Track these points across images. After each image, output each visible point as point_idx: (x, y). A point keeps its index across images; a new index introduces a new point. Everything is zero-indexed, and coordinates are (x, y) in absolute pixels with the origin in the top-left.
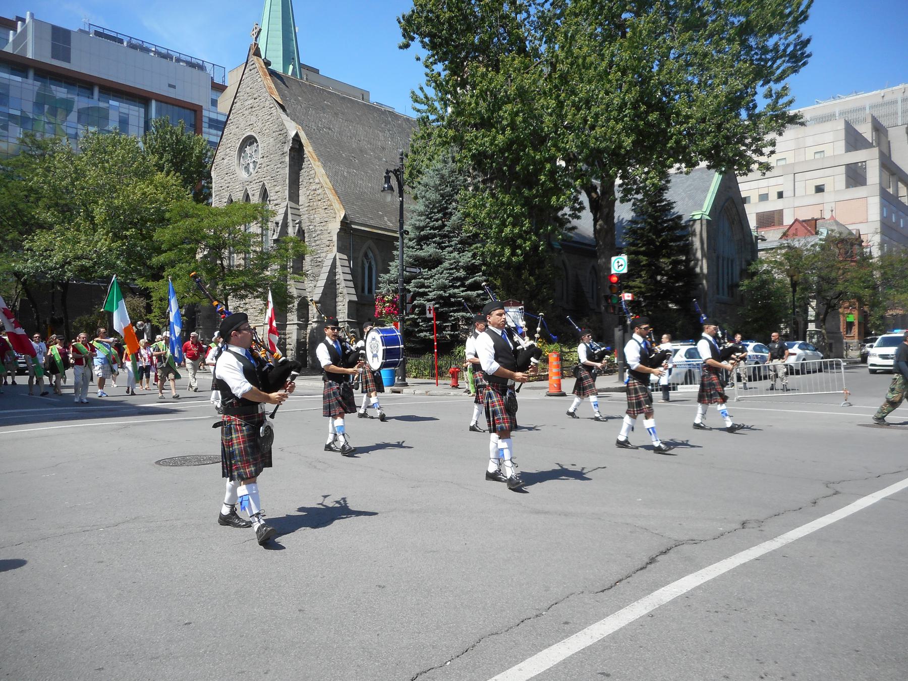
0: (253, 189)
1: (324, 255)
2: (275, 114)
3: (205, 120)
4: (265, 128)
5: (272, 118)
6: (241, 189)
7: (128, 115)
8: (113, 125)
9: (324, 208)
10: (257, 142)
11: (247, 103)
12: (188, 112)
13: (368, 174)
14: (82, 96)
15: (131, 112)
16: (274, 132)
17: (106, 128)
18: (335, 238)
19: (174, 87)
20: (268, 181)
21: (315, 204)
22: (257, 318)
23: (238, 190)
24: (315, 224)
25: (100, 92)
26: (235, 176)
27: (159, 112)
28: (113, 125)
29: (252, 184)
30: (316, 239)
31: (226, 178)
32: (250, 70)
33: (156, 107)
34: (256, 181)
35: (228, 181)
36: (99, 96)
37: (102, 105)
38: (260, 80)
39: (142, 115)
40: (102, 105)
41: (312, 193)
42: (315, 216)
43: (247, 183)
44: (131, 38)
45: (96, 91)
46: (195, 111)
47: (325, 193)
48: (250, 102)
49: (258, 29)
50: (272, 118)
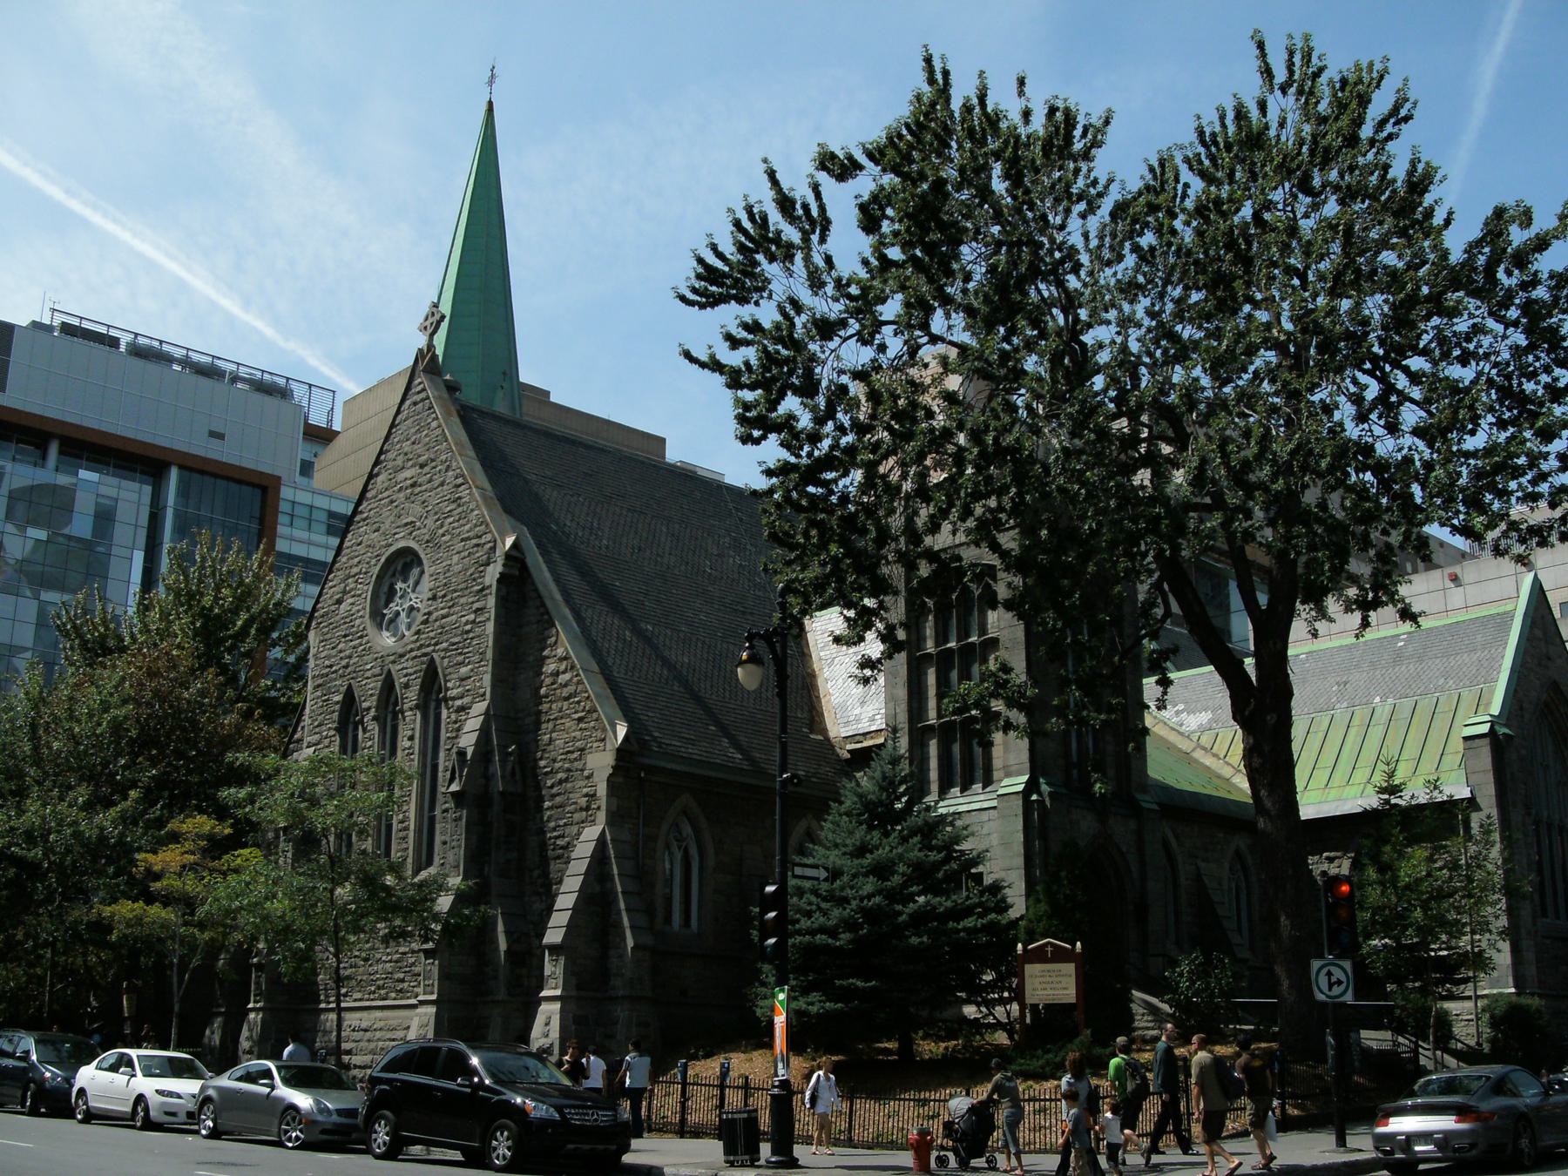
1: (574, 829)
3: (284, 507)
4: (441, 531)
5: (460, 509)
6: (377, 671)
7: (117, 500)
8: (81, 526)
9: (576, 716)
10: (420, 563)
11: (401, 476)
12: (246, 490)
13: (681, 635)
14: (21, 461)
15: (123, 494)
17: (66, 531)
18: (602, 790)
19: (221, 436)
20: (442, 654)
21: (554, 706)
22: (400, 986)
23: (368, 674)
25: (61, 452)
27: (183, 492)
28: (81, 526)
30: (555, 790)
31: (341, 646)
32: (415, 404)
33: (181, 480)
34: (414, 654)
35: (347, 653)
36: (58, 461)
37: (63, 480)
38: (434, 424)
39: (147, 499)
40: (63, 480)
42: (554, 735)
44: (136, 335)
45: (53, 450)
46: (264, 489)
47: (580, 682)
48: (408, 473)
49: (437, 317)
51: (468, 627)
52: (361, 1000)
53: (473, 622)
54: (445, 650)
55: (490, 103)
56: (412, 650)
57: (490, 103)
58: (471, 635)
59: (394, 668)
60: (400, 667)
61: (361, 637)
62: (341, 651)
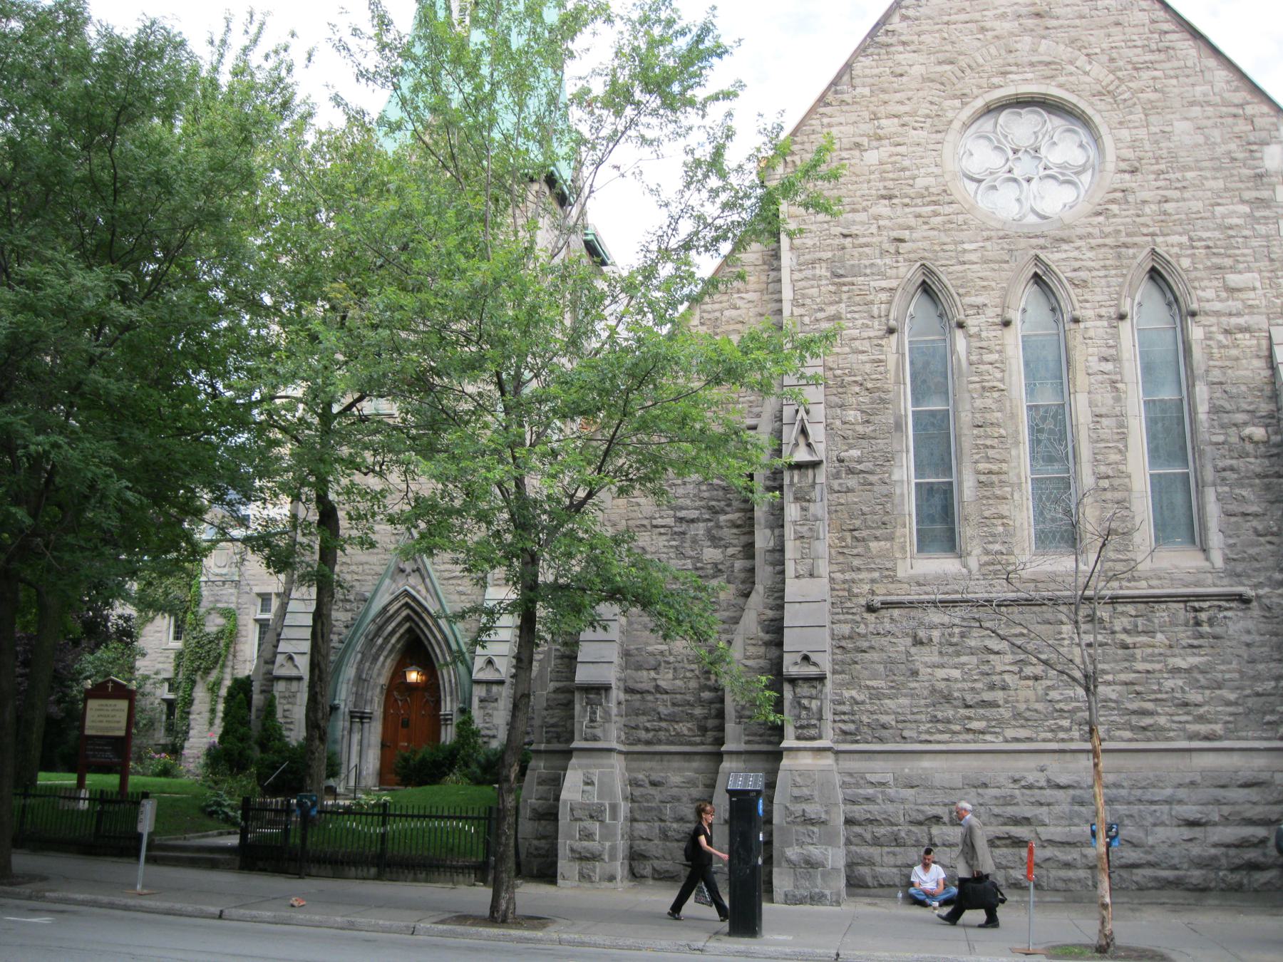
0: (1077, 264)
2: (1193, 52)
5: (1175, 64)
16: (1192, 104)
20: (1176, 250)
23: (973, 257)
26: (948, 209)
29: (1065, 246)
43: (1041, 241)
50: (1175, 64)
51: (1235, 221)
52: (1029, 739)
53: (1250, 216)
54: (1180, 245)
56: (1090, 235)
59: (1050, 257)
60: (1064, 255)
61: (935, 203)
62: (877, 217)
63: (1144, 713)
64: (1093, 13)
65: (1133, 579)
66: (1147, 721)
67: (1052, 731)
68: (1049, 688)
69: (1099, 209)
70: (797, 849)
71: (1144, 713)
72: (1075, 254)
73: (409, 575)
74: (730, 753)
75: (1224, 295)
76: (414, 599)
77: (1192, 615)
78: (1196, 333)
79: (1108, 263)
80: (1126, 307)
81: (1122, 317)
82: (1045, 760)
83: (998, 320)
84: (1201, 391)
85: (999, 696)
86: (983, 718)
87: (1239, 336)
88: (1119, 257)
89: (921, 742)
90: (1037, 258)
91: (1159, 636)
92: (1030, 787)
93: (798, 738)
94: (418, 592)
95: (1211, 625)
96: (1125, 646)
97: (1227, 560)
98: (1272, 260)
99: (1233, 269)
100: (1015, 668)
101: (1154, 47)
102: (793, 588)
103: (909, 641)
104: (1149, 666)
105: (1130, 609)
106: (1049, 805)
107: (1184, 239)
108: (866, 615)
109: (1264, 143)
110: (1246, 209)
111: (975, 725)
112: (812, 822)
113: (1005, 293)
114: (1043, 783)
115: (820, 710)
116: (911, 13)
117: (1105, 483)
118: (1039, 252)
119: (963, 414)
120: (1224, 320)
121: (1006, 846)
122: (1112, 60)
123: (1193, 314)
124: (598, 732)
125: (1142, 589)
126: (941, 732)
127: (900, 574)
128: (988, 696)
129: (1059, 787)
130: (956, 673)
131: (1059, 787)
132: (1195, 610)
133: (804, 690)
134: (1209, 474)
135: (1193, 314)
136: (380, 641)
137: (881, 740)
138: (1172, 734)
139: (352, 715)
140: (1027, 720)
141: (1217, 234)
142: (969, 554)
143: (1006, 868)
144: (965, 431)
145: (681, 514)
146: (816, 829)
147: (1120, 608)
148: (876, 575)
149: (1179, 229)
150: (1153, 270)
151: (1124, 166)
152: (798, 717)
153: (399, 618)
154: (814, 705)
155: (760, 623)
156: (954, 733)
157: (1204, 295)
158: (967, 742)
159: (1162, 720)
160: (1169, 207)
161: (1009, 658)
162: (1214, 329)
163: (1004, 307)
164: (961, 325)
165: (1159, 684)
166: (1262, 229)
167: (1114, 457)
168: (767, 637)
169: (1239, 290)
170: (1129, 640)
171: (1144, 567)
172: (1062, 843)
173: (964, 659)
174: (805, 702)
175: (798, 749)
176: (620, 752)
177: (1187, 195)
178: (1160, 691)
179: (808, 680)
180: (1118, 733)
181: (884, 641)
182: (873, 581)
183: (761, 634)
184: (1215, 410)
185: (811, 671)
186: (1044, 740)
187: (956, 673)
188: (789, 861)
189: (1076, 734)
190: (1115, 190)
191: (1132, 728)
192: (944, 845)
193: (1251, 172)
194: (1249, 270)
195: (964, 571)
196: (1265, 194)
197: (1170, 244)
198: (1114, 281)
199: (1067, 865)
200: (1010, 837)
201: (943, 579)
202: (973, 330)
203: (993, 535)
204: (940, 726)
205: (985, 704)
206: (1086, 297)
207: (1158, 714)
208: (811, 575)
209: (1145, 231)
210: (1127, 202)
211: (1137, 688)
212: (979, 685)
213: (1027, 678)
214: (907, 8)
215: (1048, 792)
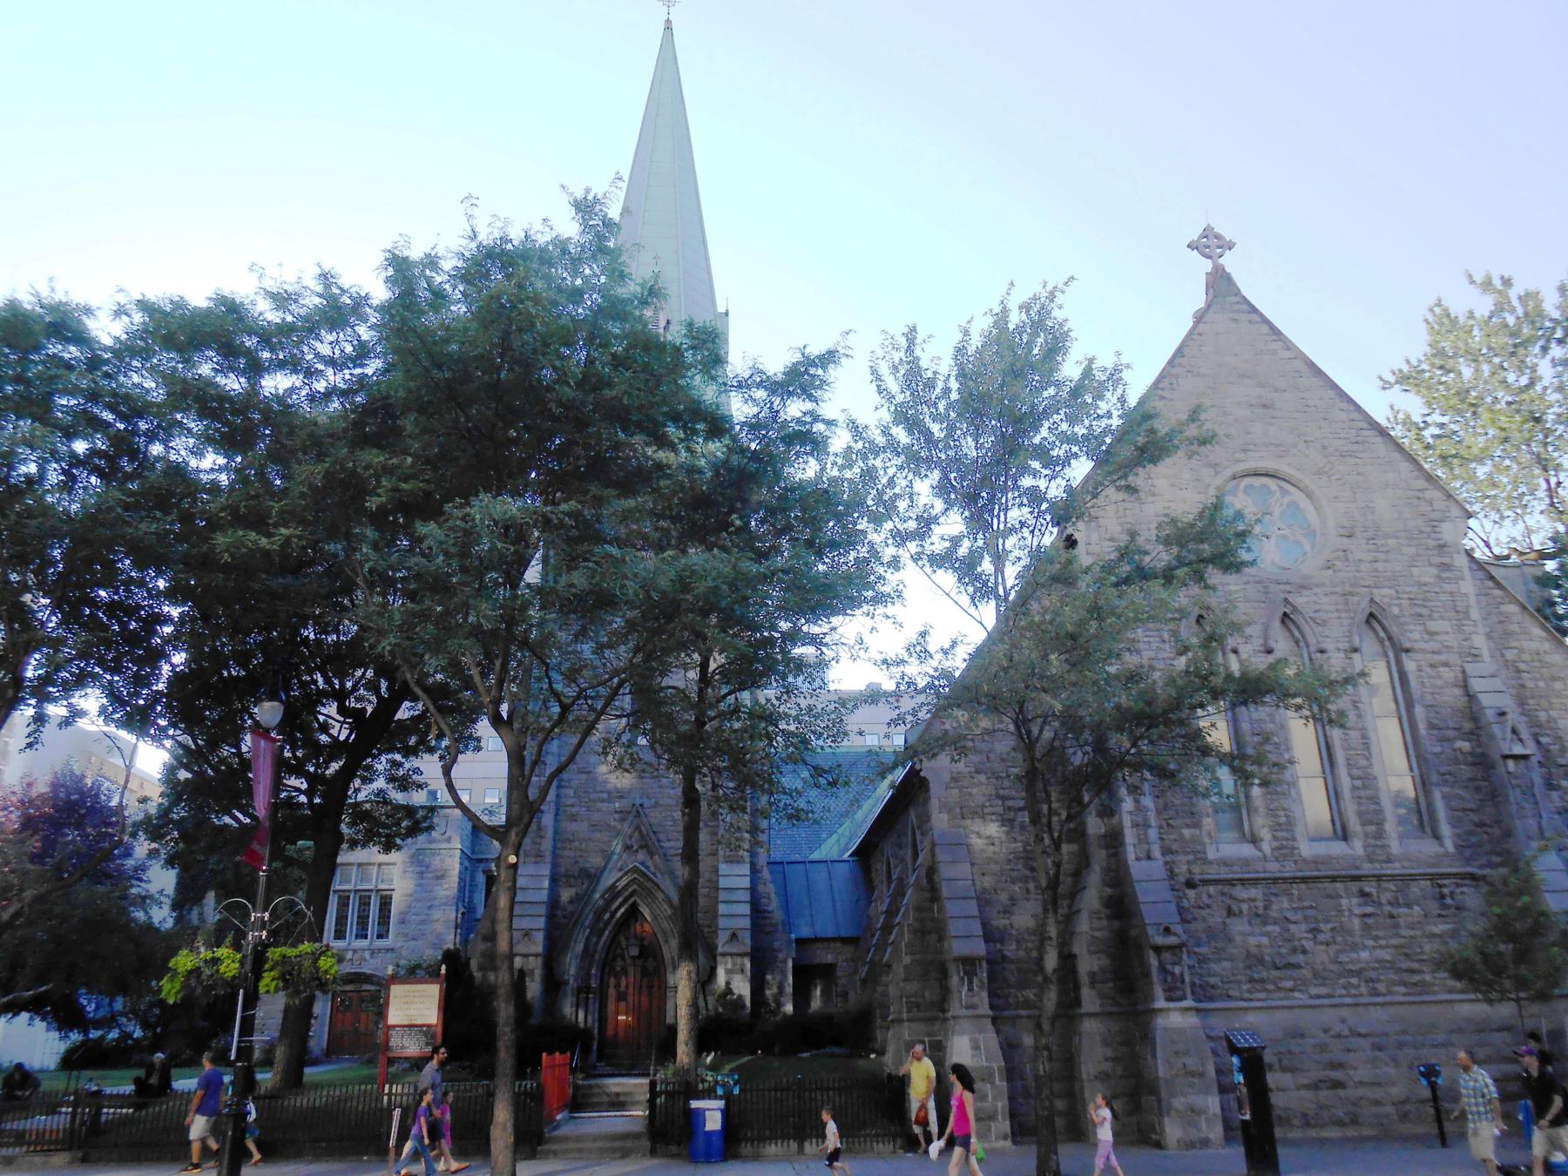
0: (1317, 607)
20: (1386, 600)
24: (1560, 733)
29: (1306, 592)
32: (1236, 320)
41: (1526, 657)
43: (1288, 588)
55: (668, 21)
56: (1323, 584)
57: (668, 21)
58: (1437, 589)
59: (1298, 600)
63: (1412, 971)
64: (1306, 409)
65: (1389, 861)
66: (1416, 978)
67: (1345, 988)
68: (1339, 952)
69: (1329, 564)
70: (1182, 1100)
71: (1412, 971)
72: (1314, 599)
73: (637, 851)
74: (1090, 1015)
75: (1426, 636)
76: (644, 875)
77: (1437, 890)
78: (1410, 665)
79: (1340, 607)
80: (1357, 643)
81: (1356, 650)
82: (1344, 1012)
83: (1262, 649)
84: (1419, 711)
85: (1300, 958)
86: (1291, 978)
87: (1441, 669)
88: (1347, 603)
89: (1245, 1000)
90: (1286, 600)
91: (1417, 908)
92: (1338, 1036)
93: (1169, 999)
94: (647, 868)
95: (1452, 899)
96: (1392, 916)
97: (1457, 847)
98: (1457, 612)
99: (1431, 617)
100: (1310, 936)
101: (1354, 440)
102: (1137, 869)
103: (1224, 913)
104: (1411, 933)
105: (1391, 886)
106: (1355, 1051)
107: (1392, 592)
108: (1188, 892)
109: (1442, 521)
110: (1434, 571)
111: (1289, 984)
112: (1192, 1074)
113: (1266, 628)
114: (1346, 1032)
115: (1182, 975)
116: (1165, 394)
117: (1358, 783)
118: (1287, 596)
119: (1243, 725)
120: (1429, 656)
121: (1327, 1088)
122: (1324, 447)
123: (1408, 651)
124: (976, 1000)
125: (1395, 869)
126: (1259, 991)
127: (1211, 854)
128: (1293, 959)
129: (1360, 1035)
130: (1265, 941)
131: (1360, 1035)
132: (1440, 886)
133: (1167, 956)
134: (1435, 778)
135: (1408, 651)
136: (607, 916)
137: (1211, 999)
138: (1436, 988)
139: (579, 990)
140: (1324, 979)
141: (1414, 589)
142: (1262, 840)
143: (1328, 1107)
144: (1248, 738)
145: (1010, 803)
146: (1195, 1080)
147: (1384, 885)
148: (1191, 857)
149: (1387, 583)
150: (1371, 615)
151: (1343, 532)
152: (1165, 980)
153: (627, 893)
154: (1177, 970)
155: (1101, 898)
156: (1267, 990)
157: (1413, 635)
158: (1281, 999)
159: (1428, 977)
160: (1380, 566)
161: (1304, 927)
162: (1422, 663)
163: (1266, 639)
164: (1235, 651)
165: (1421, 947)
166: (1447, 587)
167: (1363, 763)
168: (1108, 912)
169: (1436, 633)
170: (1394, 911)
171: (1395, 848)
172: (1373, 1084)
173: (1269, 928)
174: (1169, 967)
175: (1169, 1010)
176: (968, 1017)
177: (1391, 557)
178: (1422, 953)
179: (1171, 948)
180: (1396, 988)
181: (1204, 912)
182: (1189, 862)
183: (1104, 910)
184: (1431, 726)
185: (1172, 940)
186: (1340, 996)
187: (1265, 941)
188: (1177, 1110)
189: (1364, 990)
190: (1338, 550)
191: (1405, 985)
192: (1278, 1089)
193: (1435, 543)
194: (1442, 618)
195: (1259, 854)
196: (1446, 560)
197: (1383, 594)
198: (1346, 622)
199: (1377, 1103)
200: (1331, 1080)
201: (1245, 862)
202: (1244, 656)
203: (1279, 824)
204: (1258, 986)
205: (1290, 966)
206: (1327, 633)
207: (1423, 972)
208: (1149, 858)
209: (1363, 583)
210: (1347, 560)
211: (1406, 951)
212: (1284, 950)
213: (1322, 943)
214: (1163, 389)
215: (1353, 1040)
